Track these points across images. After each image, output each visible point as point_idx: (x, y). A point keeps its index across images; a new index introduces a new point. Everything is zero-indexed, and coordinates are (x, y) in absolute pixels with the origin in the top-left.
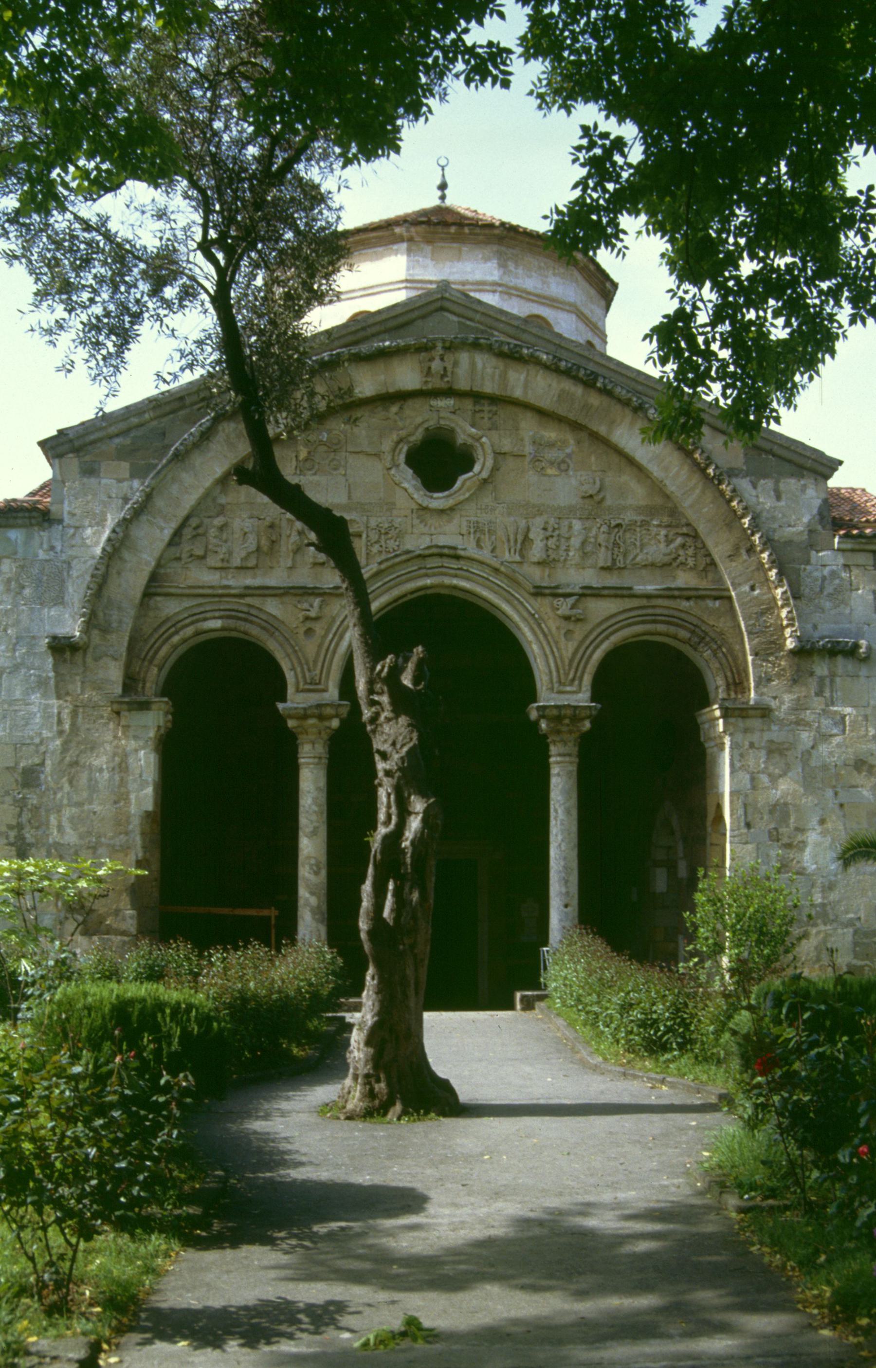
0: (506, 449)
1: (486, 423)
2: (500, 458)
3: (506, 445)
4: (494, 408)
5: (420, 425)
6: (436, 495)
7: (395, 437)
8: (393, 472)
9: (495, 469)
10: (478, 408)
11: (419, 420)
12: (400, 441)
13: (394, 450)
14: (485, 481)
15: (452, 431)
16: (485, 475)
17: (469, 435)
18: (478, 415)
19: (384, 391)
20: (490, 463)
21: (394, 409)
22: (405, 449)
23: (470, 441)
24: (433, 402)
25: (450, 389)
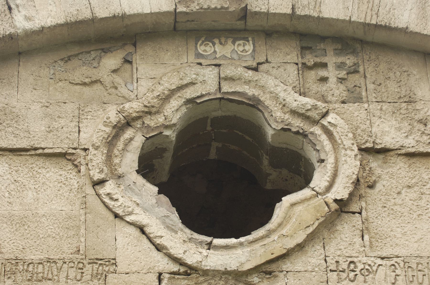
0: (387, 141)
1: (335, 89)
2: (374, 163)
3: (389, 132)
4: (349, 60)
5: (173, 92)
6: (217, 241)
7: (113, 115)
8: (109, 187)
9: (362, 185)
10: (310, 60)
11: (173, 82)
12: (128, 123)
13: (111, 142)
14: (343, 205)
15: (255, 104)
16: (341, 191)
17: (294, 113)
18: (312, 75)
19: (86, 14)
20: (350, 166)
21: (112, 61)
22: (139, 141)
23: (297, 124)
24: (205, 49)
25: (245, 14)
